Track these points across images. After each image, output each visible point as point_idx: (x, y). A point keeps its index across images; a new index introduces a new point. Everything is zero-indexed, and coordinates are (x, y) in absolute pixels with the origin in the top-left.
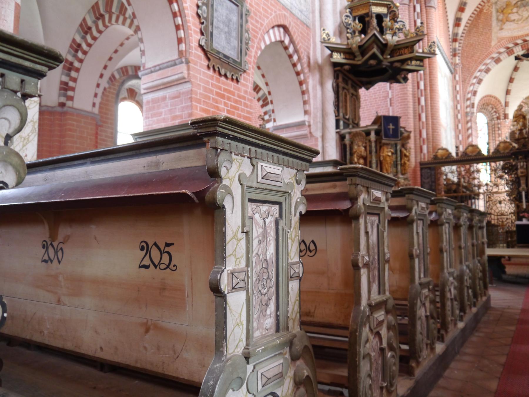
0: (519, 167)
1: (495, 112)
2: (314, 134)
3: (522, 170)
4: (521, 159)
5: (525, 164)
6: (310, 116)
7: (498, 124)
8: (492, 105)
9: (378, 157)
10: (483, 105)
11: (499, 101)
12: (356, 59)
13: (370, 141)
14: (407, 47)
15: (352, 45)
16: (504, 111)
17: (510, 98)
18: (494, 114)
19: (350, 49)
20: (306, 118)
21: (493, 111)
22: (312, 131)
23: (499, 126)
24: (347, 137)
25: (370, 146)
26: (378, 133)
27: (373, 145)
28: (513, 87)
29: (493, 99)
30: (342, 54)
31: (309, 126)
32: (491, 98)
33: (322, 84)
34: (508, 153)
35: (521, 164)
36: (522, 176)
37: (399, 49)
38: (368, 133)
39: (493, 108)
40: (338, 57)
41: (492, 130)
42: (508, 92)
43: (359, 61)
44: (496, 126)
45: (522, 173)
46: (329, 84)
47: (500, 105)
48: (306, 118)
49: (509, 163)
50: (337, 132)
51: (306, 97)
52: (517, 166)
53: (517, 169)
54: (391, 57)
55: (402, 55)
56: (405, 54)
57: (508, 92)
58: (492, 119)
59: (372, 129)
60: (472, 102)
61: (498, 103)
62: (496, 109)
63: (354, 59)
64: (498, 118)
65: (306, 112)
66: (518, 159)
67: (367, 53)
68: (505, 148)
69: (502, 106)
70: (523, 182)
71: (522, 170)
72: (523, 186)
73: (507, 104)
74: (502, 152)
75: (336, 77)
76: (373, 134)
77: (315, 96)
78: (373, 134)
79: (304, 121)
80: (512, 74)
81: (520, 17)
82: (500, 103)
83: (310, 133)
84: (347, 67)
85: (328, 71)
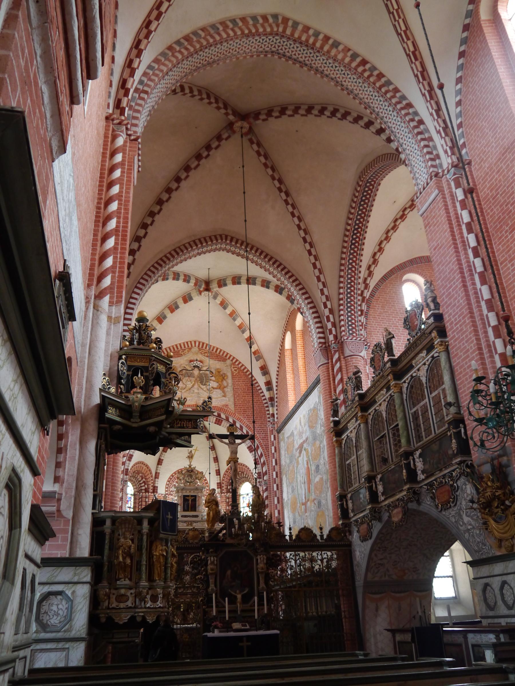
0: (209, 562)
1: (144, 482)
2: (64, 513)
3: (212, 567)
4: (212, 552)
5: (215, 559)
6: (62, 485)
7: (146, 497)
8: (142, 473)
9: (150, 556)
11: (150, 470)
12: (132, 420)
13: (140, 532)
14: (190, 420)
15: (134, 402)
16: (154, 483)
17: (162, 469)
18: (143, 484)
19: (130, 406)
20: (56, 488)
22: (62, 507)
24: (108, 522)
25: (141, 540)
26: (151, 522)
27: (145, 538)
29: (145, 467)
30: (118, 411)
31: (59, 500)
32: (143, 466)
33: (82, 442)
34: (197, 543)
35: (211, 559)
36: (211, 574)
37: (180, 420)
38: (140, 521)
39: (142, 479)
40: (111, 414)
43: (135, 423)
44: (144, 499)
45: (212, 569)
46: (92, 446)
47: (150, 475)
48: (56, 488)
49: (198, 556)
50: (93, 513)
51: (61, 458)
52: (208, 561)
53: (206, 565)
54: (170, 427)
55: (183, 427)
56: (187, 427)
58: (140, 491)
59: (146, 517)
60: (126, 467)
61: (148, 472)
63: (129, 420)
64: (147, 490)
65: (57, 479)
66: (208, 552)
67: (150, 418)
68: (194, 538)
69: (152, 476)
70: (212, 581)
71: (212, 567)
72: (212, 586)
73: (157, 476)
74: (191, 541)
75: (99, 438)
76: (145, 524)
77: (73, 458)
78: (145, 524)
79: (55, 492)
81: (184, 386)
82: (151, 473)
83: (59, 511)
84: (118, 427)
85: (92, 426)
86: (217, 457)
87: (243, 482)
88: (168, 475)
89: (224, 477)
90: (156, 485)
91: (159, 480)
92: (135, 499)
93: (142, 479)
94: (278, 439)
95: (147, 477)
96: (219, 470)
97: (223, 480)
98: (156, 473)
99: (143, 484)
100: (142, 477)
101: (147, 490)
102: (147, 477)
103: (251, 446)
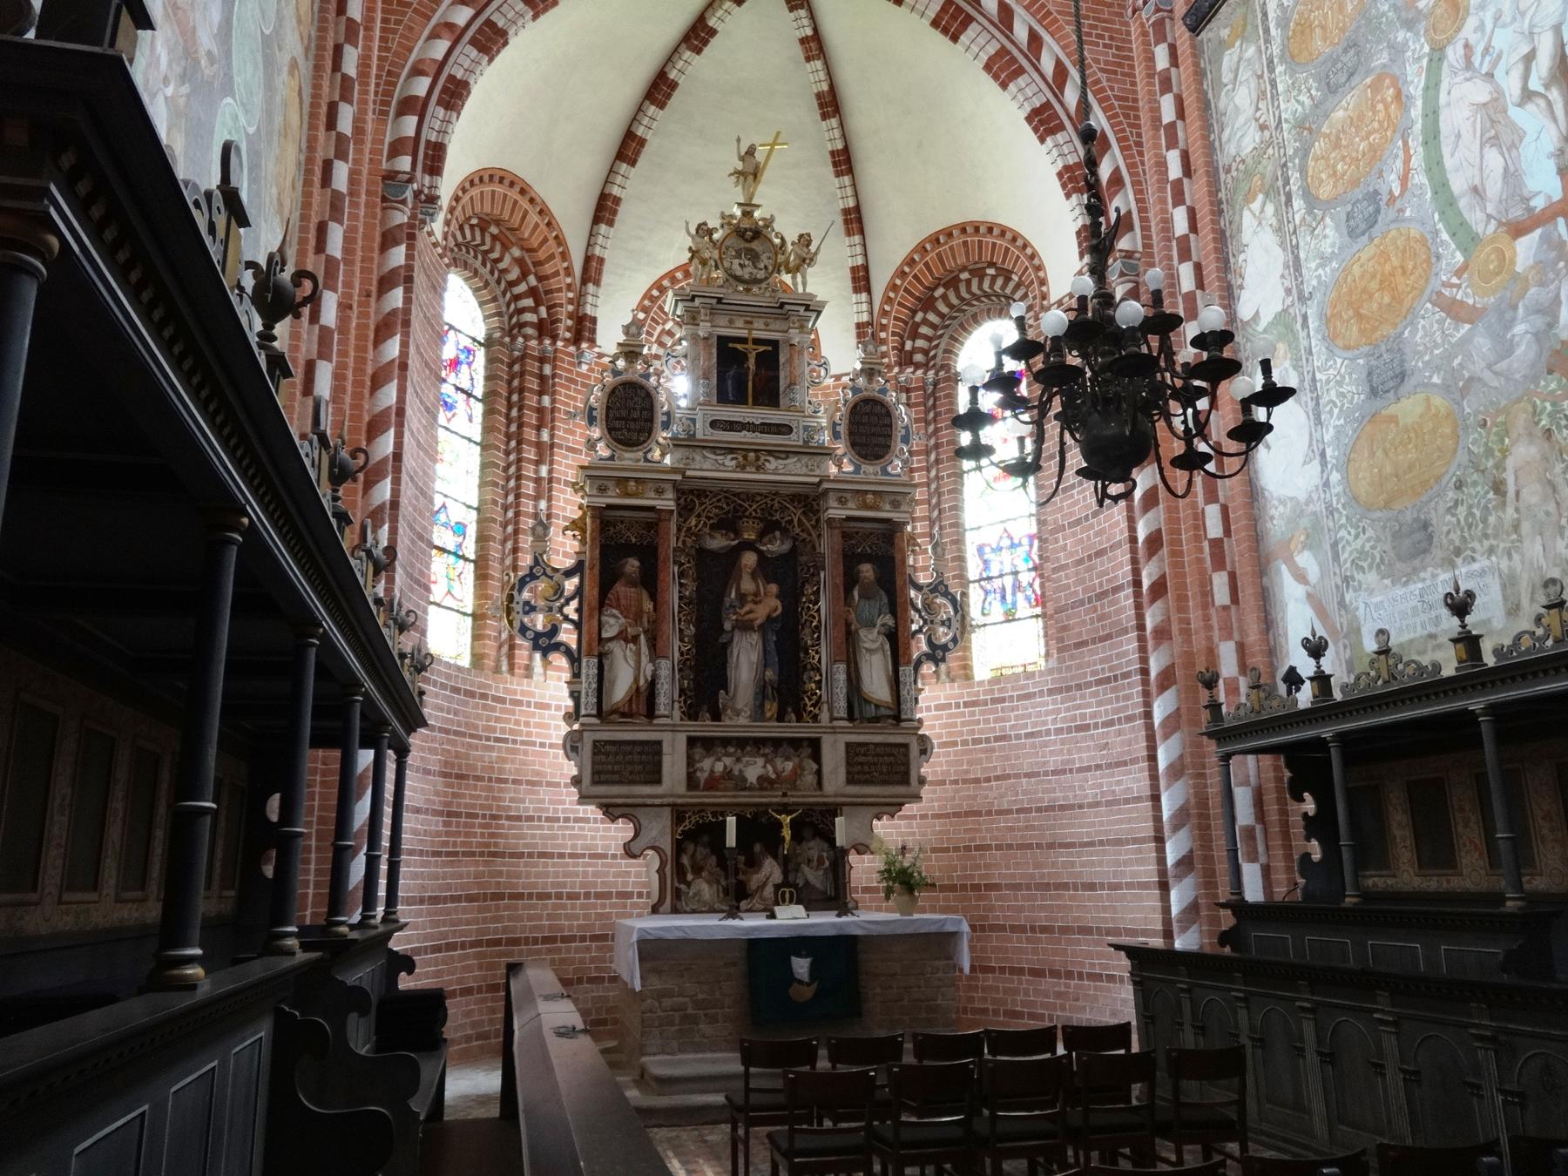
1: (532, 292)
7: (542, 360)
10: (483, 226)
11: (559, 240)
16: (579, 301)
17: (612, 244)
18: (528, 302)
21: (522, 288)
23: (547, 370)
28: (632, 185)
29: (534, 217)
41: (509, 383)
42: (605, 209)
44: (532, 366)
57: (605, 209)
58: (514, 330)
62: (540, 279)
69: (569, 272)
73: (592, 270)
80: (672, 55)
82: (565, 256)
86: (857, 209)
87: (976, 320)
88: (641, 282)
89: (888, 300)
90: (589, 310)
91: (601, 291)
92: (491, 361)
93: (524, 275)
94: (1196, 52)
95: (548, 269)
96: (866, 268)
97: (884, 313)
98: (588, 259)
99: (529, 302)
100: (520, 262)
101: (545, 329)
102: (548, 269)
103: (1047, 105)
